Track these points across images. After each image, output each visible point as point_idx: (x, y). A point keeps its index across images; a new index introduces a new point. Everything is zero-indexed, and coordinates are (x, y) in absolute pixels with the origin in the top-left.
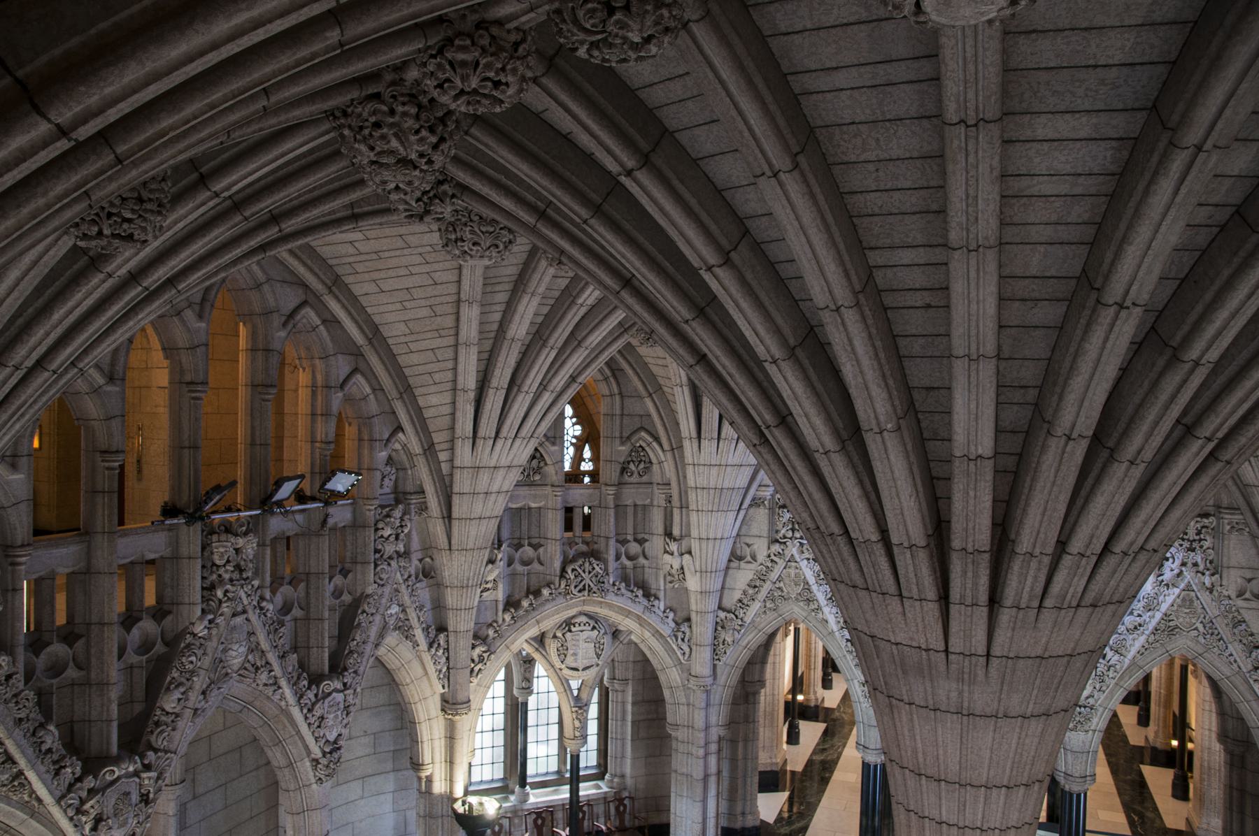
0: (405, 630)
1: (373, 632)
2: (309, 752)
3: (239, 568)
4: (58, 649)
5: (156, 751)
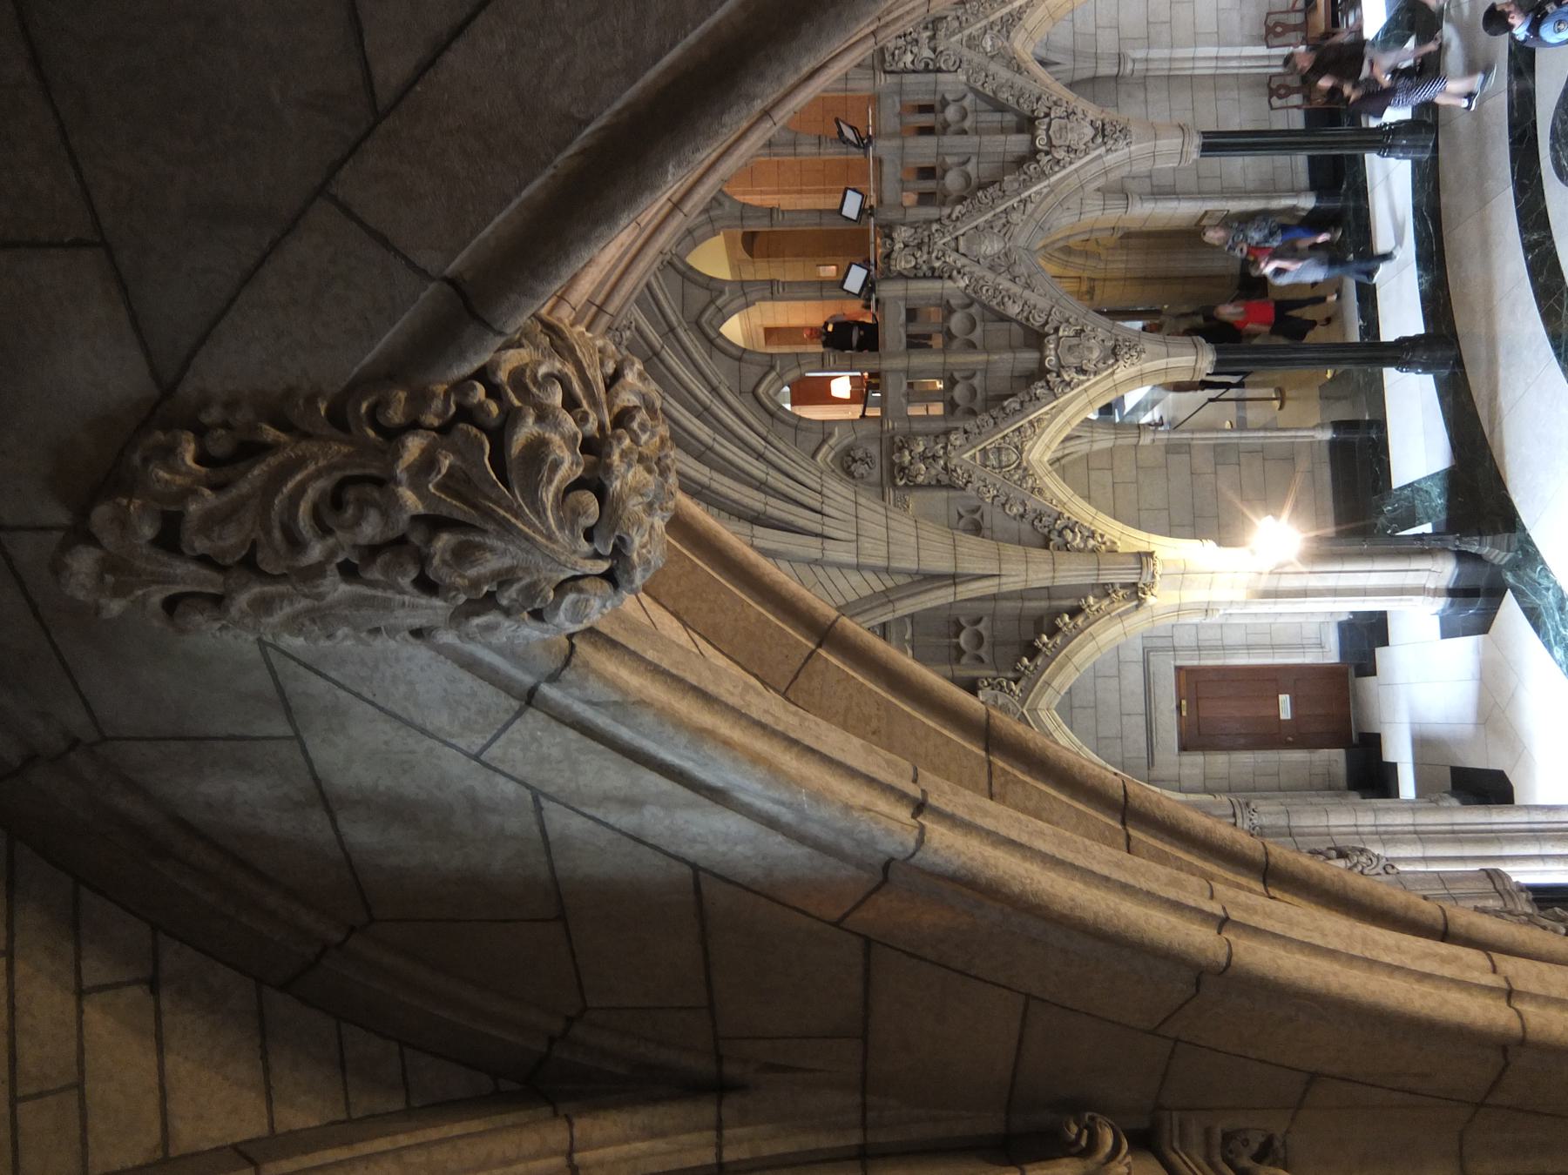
0: (1011, 22)
1: (1004, 74)
2: (1100, 157)
3: (919, 247)
4: (959, 392)
5: (1047, 323)
